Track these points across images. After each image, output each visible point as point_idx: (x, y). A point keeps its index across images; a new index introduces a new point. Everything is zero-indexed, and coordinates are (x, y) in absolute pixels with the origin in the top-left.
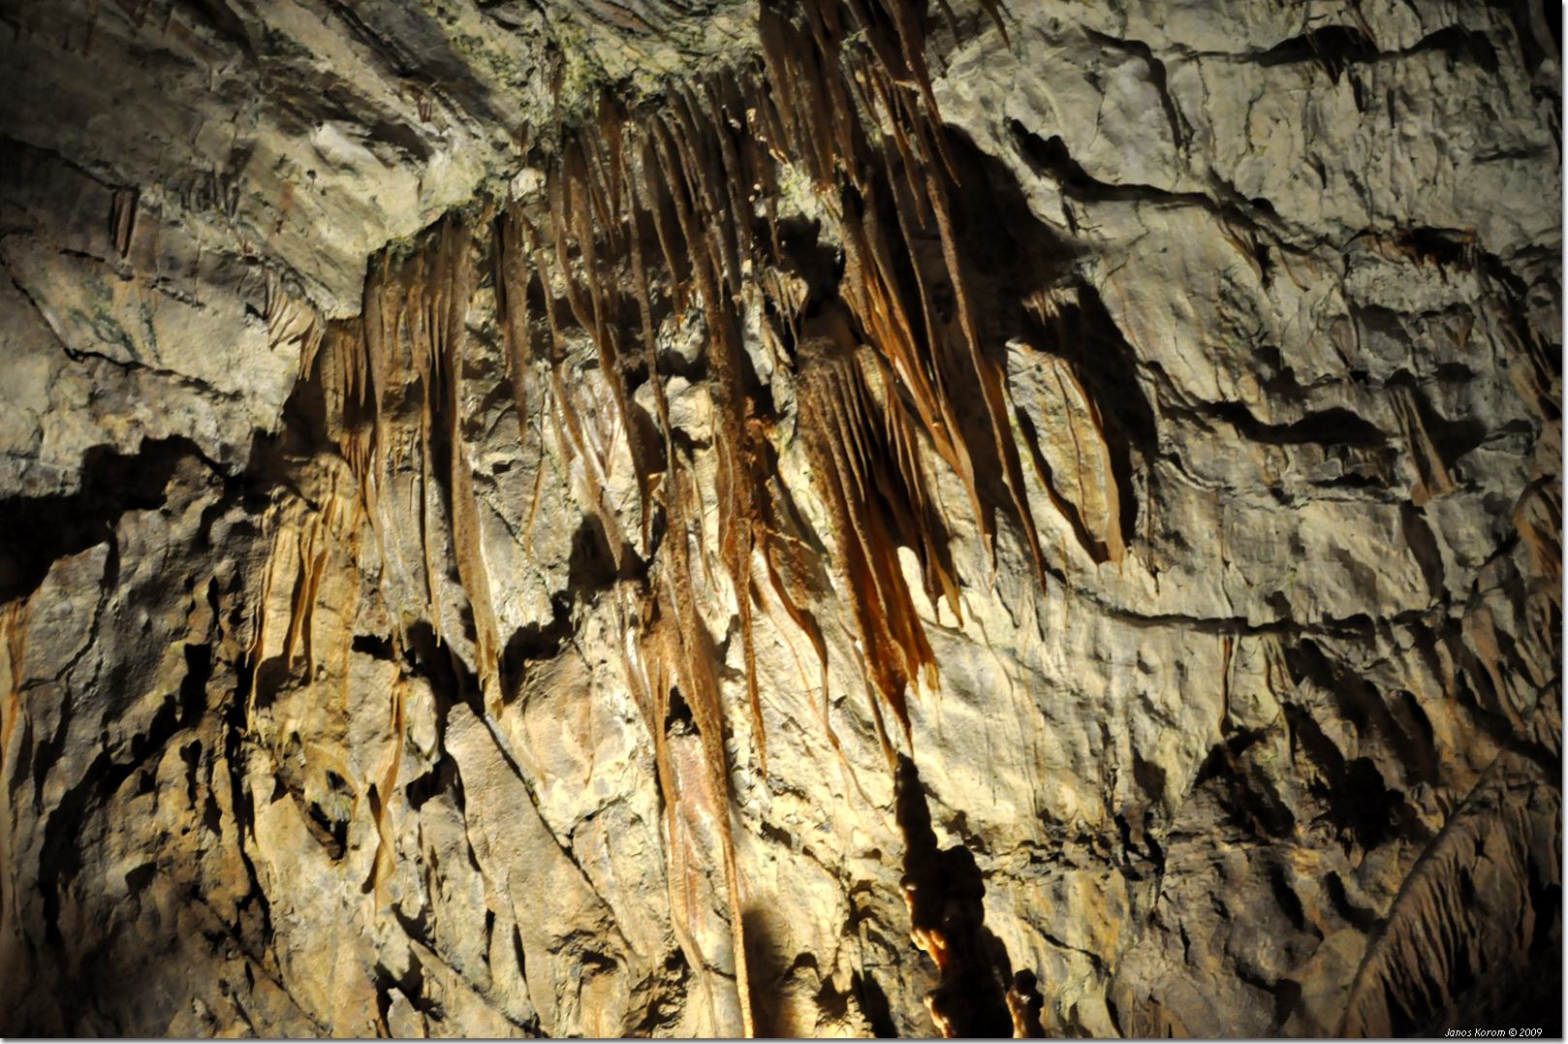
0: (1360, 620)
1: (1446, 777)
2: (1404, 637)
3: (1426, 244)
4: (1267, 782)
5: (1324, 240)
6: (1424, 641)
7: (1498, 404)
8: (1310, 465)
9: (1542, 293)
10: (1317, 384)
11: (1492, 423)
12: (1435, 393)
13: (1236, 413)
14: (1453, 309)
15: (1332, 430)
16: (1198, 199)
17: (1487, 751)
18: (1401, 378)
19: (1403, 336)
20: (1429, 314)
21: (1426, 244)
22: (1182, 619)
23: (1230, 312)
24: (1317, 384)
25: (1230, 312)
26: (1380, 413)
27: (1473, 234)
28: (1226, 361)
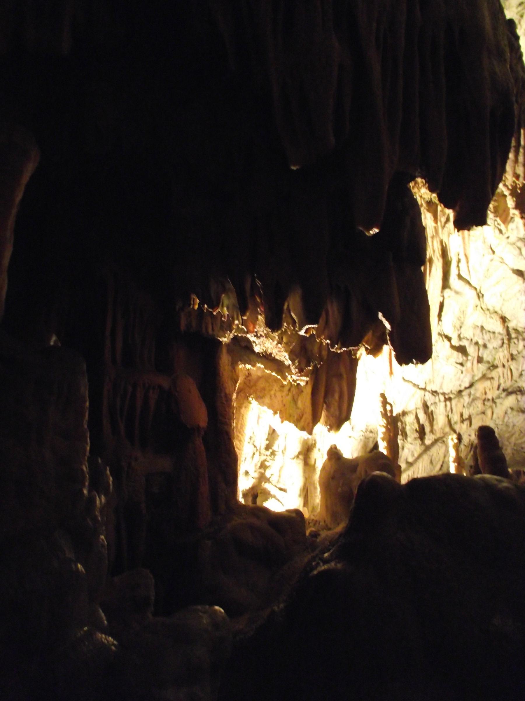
0: (436, 392)
1: (434, 432)
2: (442, 398)
3: (504, 319)
4: (406, 425)
5: (488, 310)
6: (446, 400)
7: (488, 356)
8: (458, 358)
9: (516, 341)
10: (464, 338)
11: (485, 359)
12: (481, 349)
13: (449, 339)
14: (494, 333)
15: (462, 350)
16: (476, 289)
17: (447, 429)
18: (477, 343)
19: (483, 334)
20: (489, 332)
21: (504, 319)
22: (411, 382)
23: (462, 316)
24: (464, 338)
25: (462, 316)
26: (471, 350)
27: (509, 320)
28: (455, 327)
